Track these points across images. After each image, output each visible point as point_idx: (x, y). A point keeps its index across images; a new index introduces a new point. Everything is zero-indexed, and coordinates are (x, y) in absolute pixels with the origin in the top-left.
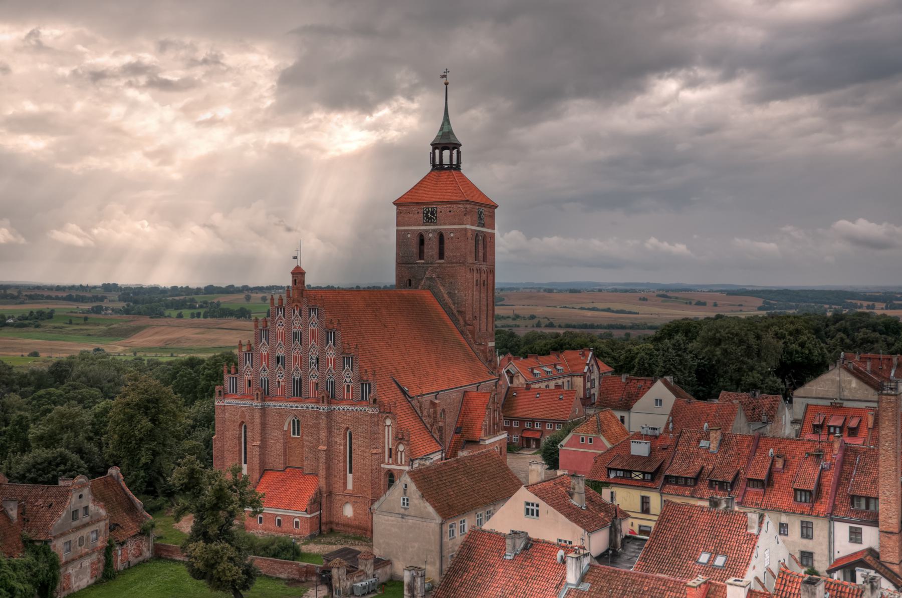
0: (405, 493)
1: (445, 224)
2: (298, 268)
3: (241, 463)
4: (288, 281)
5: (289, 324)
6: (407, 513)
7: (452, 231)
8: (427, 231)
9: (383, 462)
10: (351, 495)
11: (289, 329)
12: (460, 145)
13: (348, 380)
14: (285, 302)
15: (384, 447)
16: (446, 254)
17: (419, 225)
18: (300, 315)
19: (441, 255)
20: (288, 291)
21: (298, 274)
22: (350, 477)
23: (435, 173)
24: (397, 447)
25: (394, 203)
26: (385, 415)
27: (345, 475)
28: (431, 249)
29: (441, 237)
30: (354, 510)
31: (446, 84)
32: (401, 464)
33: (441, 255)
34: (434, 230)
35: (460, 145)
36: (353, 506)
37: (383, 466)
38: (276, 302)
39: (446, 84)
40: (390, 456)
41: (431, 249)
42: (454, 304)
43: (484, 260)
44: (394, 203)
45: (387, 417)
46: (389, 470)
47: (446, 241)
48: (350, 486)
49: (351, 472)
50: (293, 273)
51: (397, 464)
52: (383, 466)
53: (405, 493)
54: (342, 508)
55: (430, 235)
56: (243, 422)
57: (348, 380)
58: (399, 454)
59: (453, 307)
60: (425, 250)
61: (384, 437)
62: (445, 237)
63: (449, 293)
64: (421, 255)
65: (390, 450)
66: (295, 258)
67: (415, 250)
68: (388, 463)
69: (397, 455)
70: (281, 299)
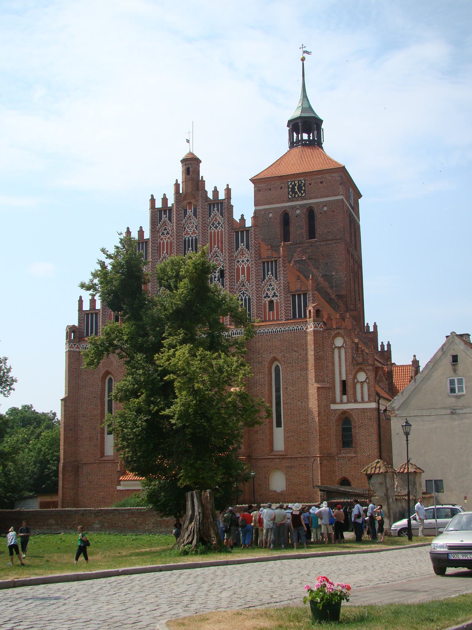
0: (455, 371)
1: (316, 198)
2: (191, 153)
3: (104, 433)
4: (177, 174)
5: (181, 228)
6: (461, 403)
7: (325, 204)
8: (293, 207)
9: (334, 402)
10: (282, 457)
11: (178, 236)
12: (321, 121)
13: (271, 294)
14: (171, 202)
15: (334, 381)
16: (319, 230)
17: (283, 202)
18: (195, 214)
19: (312, 233)
20: (177, 185)
21: (191, 165)
22: (279, 434)
23: (297, 150)
24: (355, 377)
25: (252, 180)
26: (333, 333)
27: (272, 428)
28: (299, 228)
29: (311, 213)
30: (287, 480)
31: (303, 59)
32: (363, 401)
33: (312, 233)
34: (301, 206)
35: (322, 121)
36: (286, 474)
37: (333, 407)
38: (159, 204)
39: (303, 59)
40: (344, 391)
41: (299, 228)
42: (332, 287)
43: (356, 249)
44: (252, 180)
45: (338, 335)
46: (344, 412)
47: (318, 216)
48: (279, 444)
49: (279, 425)
50: (183, 161)
51: (356, 401)
52: (333, 407)
53: (455, 371)
54: (267, 479)
55: (298, 212)
56: (108, 373)
57: (271, 294)
58: (358, 386)
59: (330, 291)
60: (292, 229)
61: (333, 364)
62: (316, 211)
63: (324, 276)
64: (286, 237)
65: (344, 383)
66: (188, 141)
67: (278, 230)
68: (342, 402)
69: (355, 388)
70: (165, 200)
